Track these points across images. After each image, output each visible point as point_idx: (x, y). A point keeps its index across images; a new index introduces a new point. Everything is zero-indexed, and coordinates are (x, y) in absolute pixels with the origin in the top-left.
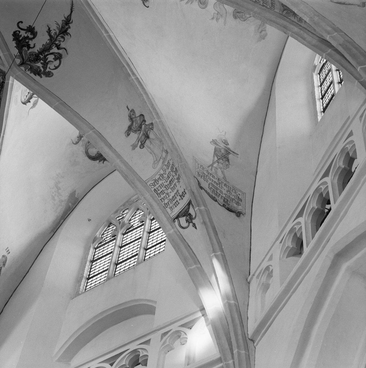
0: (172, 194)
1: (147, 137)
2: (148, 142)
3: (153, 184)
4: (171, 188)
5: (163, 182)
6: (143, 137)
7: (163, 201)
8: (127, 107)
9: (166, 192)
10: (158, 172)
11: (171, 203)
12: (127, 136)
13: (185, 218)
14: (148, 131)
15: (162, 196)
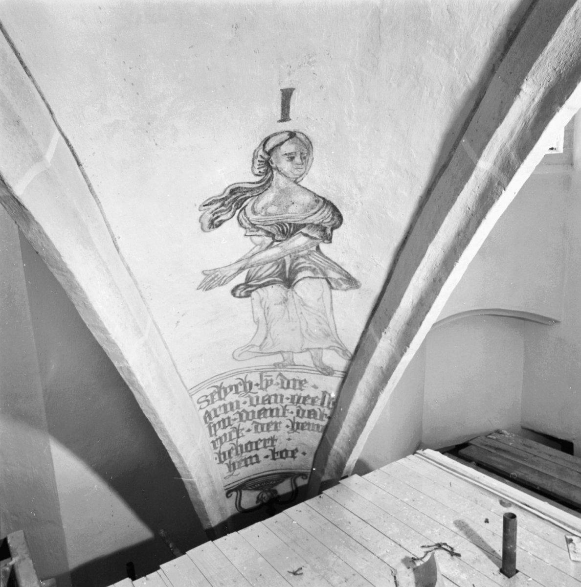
0: (253, 437)
1: (288, 280)
2: (275, 292)
3: (209, 398)
4: (254, 422)
5: (242, 400)
6: (268, 270)
7: (218, 445)
8: (287, 95)
9: (236, 424)
10: (242, 372)
11: (237, 454)
12: (206, 223)
13: (257, 493)
14: (306, 268)
15: (220, 433)
